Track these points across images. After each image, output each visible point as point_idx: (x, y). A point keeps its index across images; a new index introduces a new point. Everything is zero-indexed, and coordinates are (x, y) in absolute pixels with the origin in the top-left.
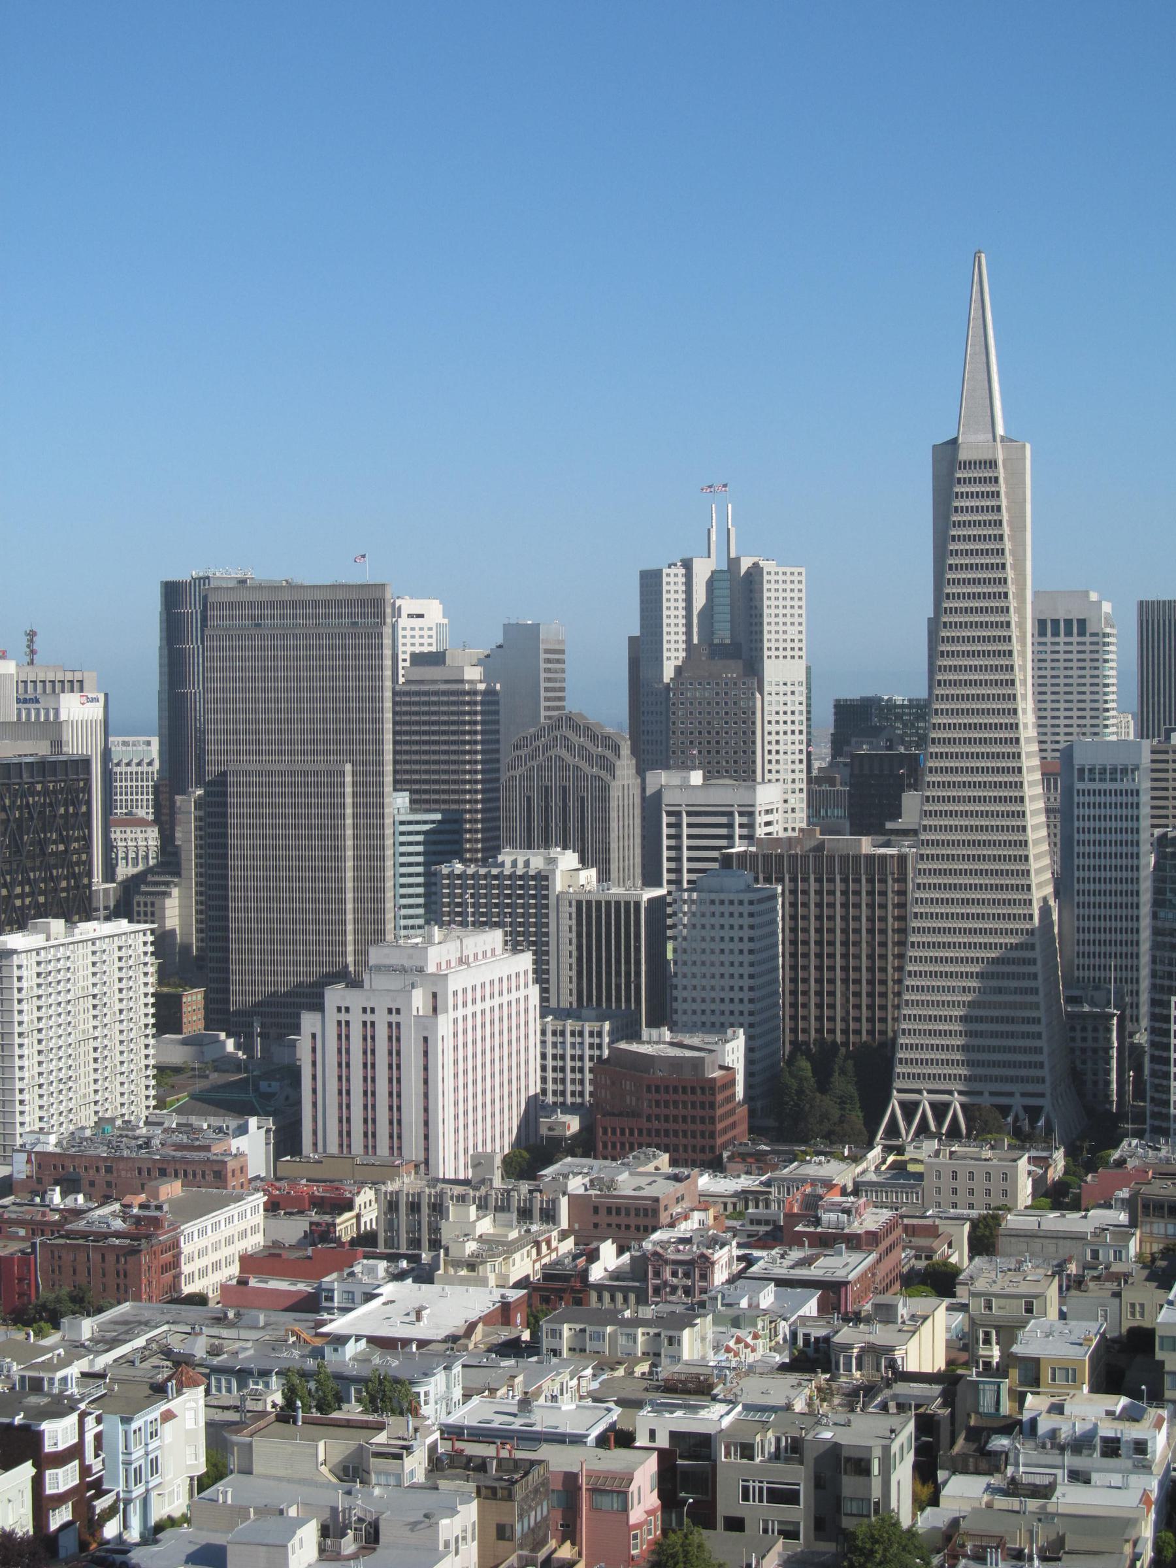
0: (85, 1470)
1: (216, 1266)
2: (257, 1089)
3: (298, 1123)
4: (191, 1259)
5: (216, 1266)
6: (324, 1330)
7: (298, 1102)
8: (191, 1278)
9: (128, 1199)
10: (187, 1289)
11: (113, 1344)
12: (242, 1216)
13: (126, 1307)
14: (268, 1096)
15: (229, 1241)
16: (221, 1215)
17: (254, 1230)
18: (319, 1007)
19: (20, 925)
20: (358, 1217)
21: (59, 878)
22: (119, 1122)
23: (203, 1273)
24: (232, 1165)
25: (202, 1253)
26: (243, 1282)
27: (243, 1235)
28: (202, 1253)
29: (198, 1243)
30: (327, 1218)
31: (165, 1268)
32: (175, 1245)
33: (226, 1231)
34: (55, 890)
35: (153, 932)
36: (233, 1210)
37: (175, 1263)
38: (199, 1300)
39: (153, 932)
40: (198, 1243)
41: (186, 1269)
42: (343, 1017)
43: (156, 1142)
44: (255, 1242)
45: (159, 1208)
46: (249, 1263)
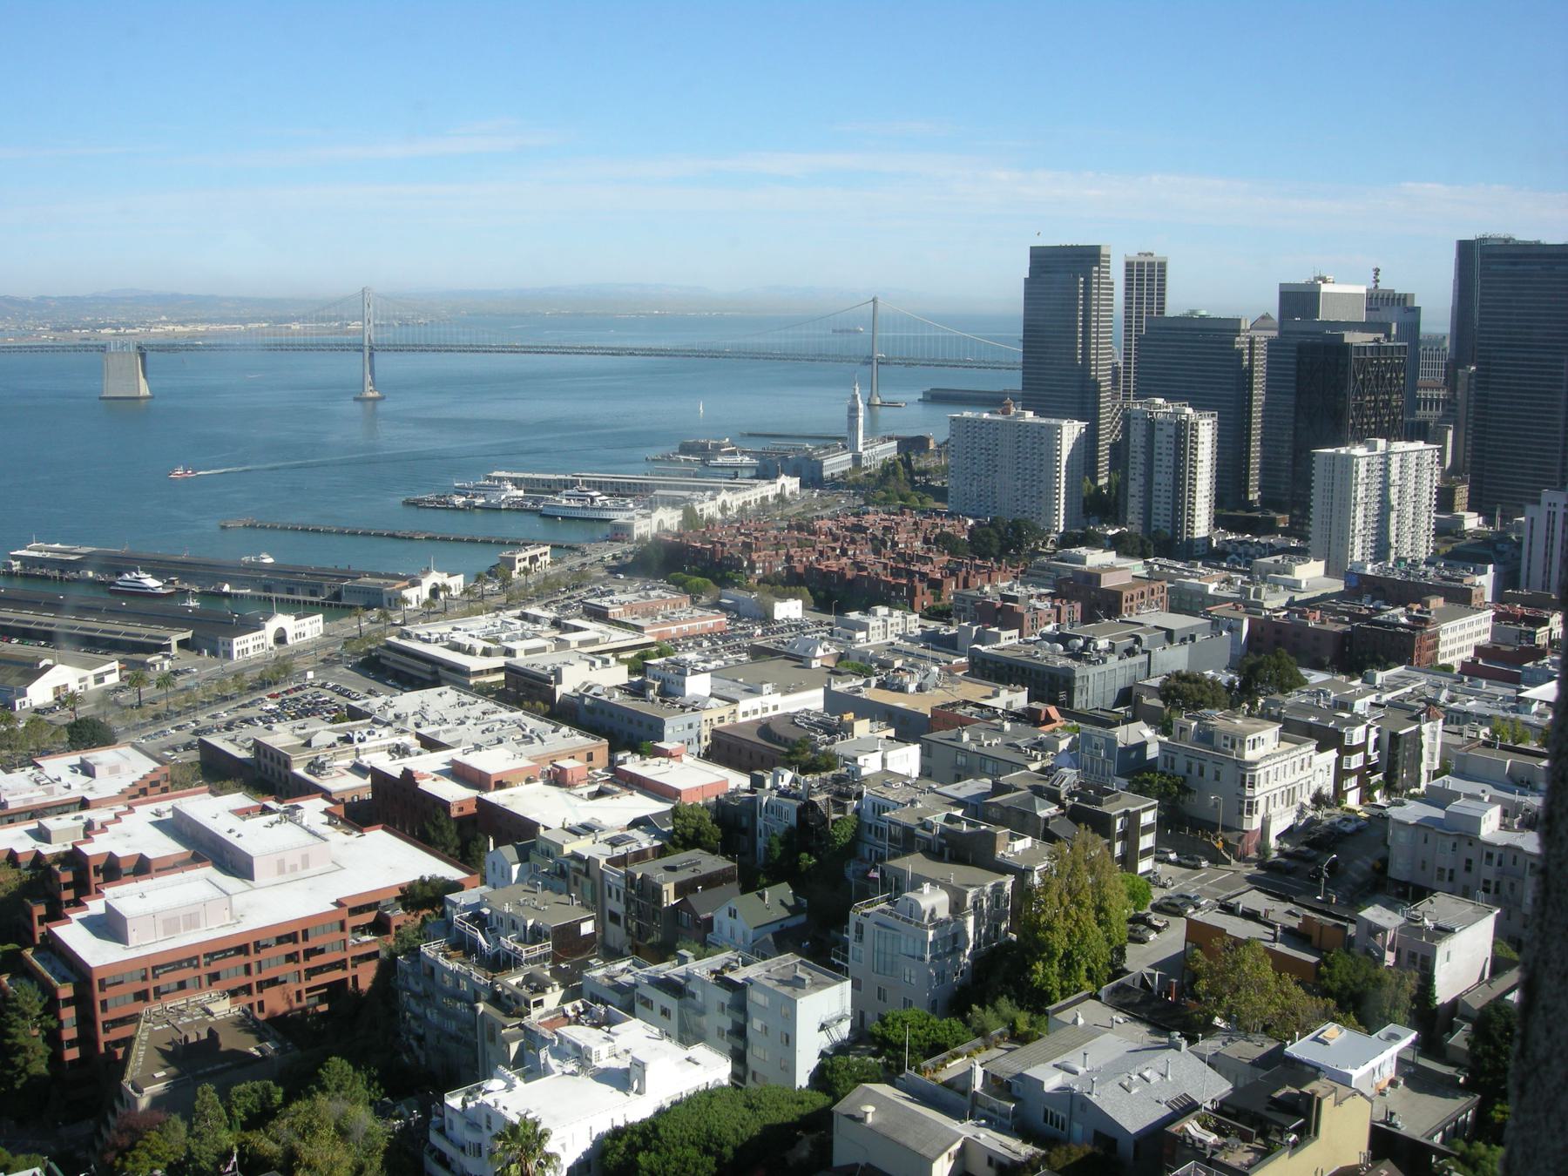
0: (1367, 758)
1: (1461, 650)
2: (1494, 548)
3: (1518, 570)
4: (1445, 643)
5: (1461, 650)
6: (1522, 695)
7: (1520, 558)
8: (1444, 655)
9: (1410, 605)
10: (1441, 662)
11: (1395, 688)
12: (1479, 622)
13: (1400, 669)
14: (1501, 553)
15: (1470, 636)
16: (1465, 620)
17: (1486, 631)
18: (1538, 503)
19: (1360, 438)
20: (1551, 630)
21: (1384, 416)
22: (1409, 561)
23: (1452, 653)
24: (1475, 591)
25: (1453, 641)
26: (1475, 662)
27: (1478, 634)
28: (1453, 641)
29: (1451, 636)
30: (1531, 629)
31: (1429, 648)
32: (1436, 635)
33: (1469, 630)
34: (1381, 422)
35: (1439, 450)
36: (1473, 618)
37: (1436, 645)
38: (1447, 668)
39: (1439, 450)
40: (1451, 636)
41: (1442, 649)
42: (1552, 509)
43: (1431, 574)
44: (1485, 638)
45: (1429, 613)
46: (1479, 650)
